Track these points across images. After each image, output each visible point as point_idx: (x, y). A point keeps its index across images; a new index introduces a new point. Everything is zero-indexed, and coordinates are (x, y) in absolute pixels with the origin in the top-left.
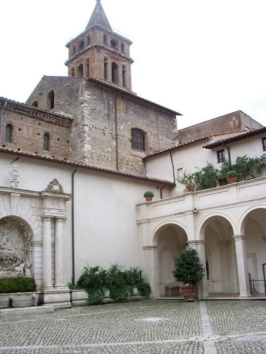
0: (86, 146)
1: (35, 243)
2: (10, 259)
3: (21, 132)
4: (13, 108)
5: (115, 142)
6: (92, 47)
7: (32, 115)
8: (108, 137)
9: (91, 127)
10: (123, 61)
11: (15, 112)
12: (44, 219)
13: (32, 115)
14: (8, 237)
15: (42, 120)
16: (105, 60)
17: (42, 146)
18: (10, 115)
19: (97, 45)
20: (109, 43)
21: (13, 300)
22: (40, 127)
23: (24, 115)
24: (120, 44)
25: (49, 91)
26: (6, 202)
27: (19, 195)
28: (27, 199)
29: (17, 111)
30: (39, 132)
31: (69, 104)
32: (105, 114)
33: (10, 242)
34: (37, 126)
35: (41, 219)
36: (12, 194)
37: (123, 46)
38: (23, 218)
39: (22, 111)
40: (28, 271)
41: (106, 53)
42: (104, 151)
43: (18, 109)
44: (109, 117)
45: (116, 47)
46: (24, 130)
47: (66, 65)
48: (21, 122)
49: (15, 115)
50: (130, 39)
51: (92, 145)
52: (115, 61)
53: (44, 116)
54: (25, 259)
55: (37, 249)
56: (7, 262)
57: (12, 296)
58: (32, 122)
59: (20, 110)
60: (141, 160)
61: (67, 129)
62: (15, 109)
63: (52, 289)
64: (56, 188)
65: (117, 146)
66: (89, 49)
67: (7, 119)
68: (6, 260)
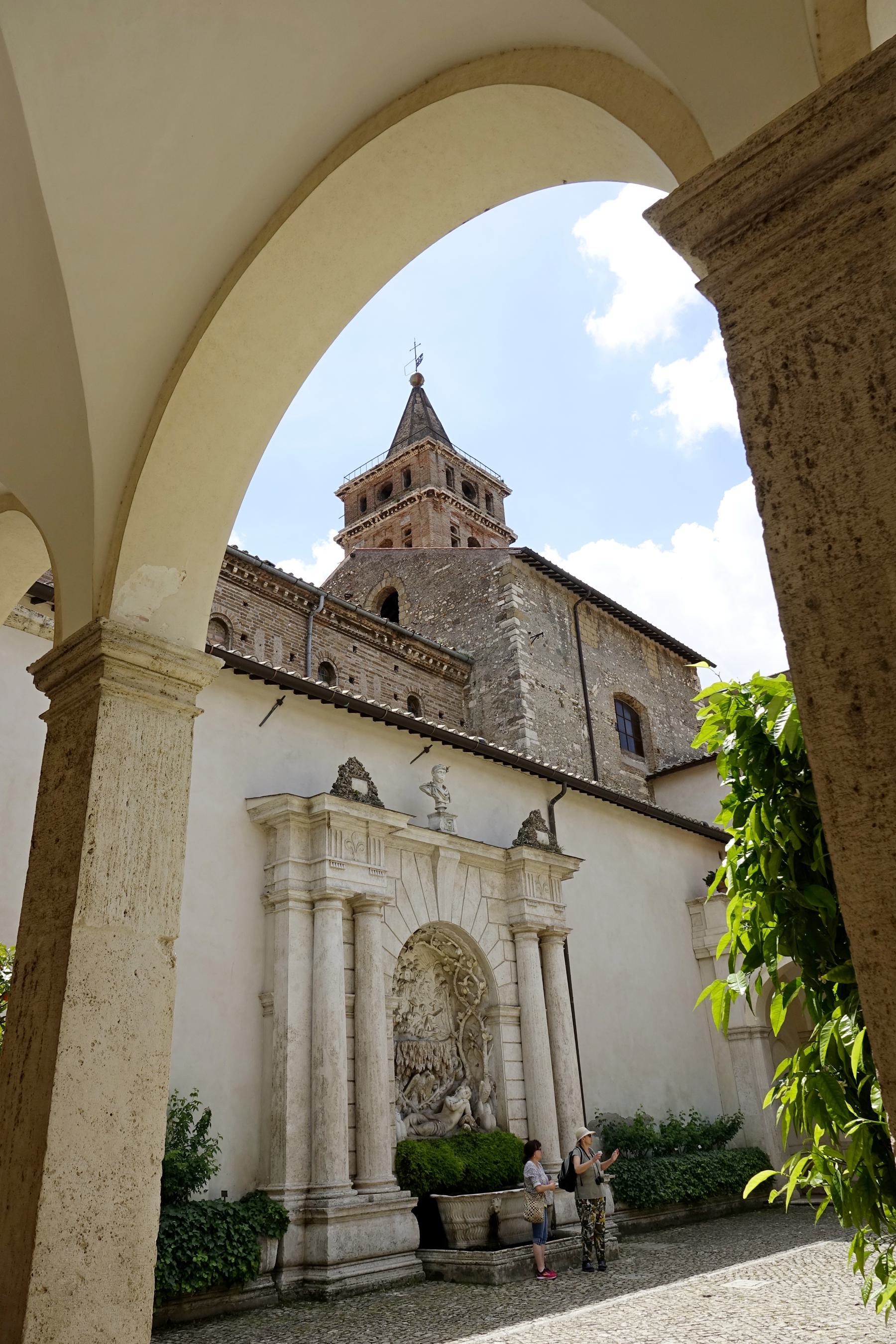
0: (529, 733)
5: (586, 727)
6: (420, 497)
7: (378, 641)
8: (568, 716)
9: (534, 682)
10: (494, 537)
11: (339, 630)
13: (378, 641)
15: (402, 658)
16: (453, 529)
18: (327, 638)
19: (433, 491)
20: (459, 487)
21: (500, 1216)
22: (398, 678)
24: (483, 494)
25: (379, 589)
27: (458, 856)
31: (456, 622)
32: (558, 651)
34: (390, 675)
37: (489, 498)
39: (355, 626)
40: (486, 1110)
41: (454, 514)
42: (565, 751)
43: (348, 623)
44: (566, 659)
45: (475, 501)
47: (339, 542)
48: (354, 659)
50: (508, 484)
51: (540, 734)
52: (474, 535)
53: (406, 648)
54: (463, 1069)
55: (508, 1033)
58: (378, 661)
60: (642, 780)
61: (457, 688)
62: (339, 620)
65: (591, 739)
66: (412, 500)
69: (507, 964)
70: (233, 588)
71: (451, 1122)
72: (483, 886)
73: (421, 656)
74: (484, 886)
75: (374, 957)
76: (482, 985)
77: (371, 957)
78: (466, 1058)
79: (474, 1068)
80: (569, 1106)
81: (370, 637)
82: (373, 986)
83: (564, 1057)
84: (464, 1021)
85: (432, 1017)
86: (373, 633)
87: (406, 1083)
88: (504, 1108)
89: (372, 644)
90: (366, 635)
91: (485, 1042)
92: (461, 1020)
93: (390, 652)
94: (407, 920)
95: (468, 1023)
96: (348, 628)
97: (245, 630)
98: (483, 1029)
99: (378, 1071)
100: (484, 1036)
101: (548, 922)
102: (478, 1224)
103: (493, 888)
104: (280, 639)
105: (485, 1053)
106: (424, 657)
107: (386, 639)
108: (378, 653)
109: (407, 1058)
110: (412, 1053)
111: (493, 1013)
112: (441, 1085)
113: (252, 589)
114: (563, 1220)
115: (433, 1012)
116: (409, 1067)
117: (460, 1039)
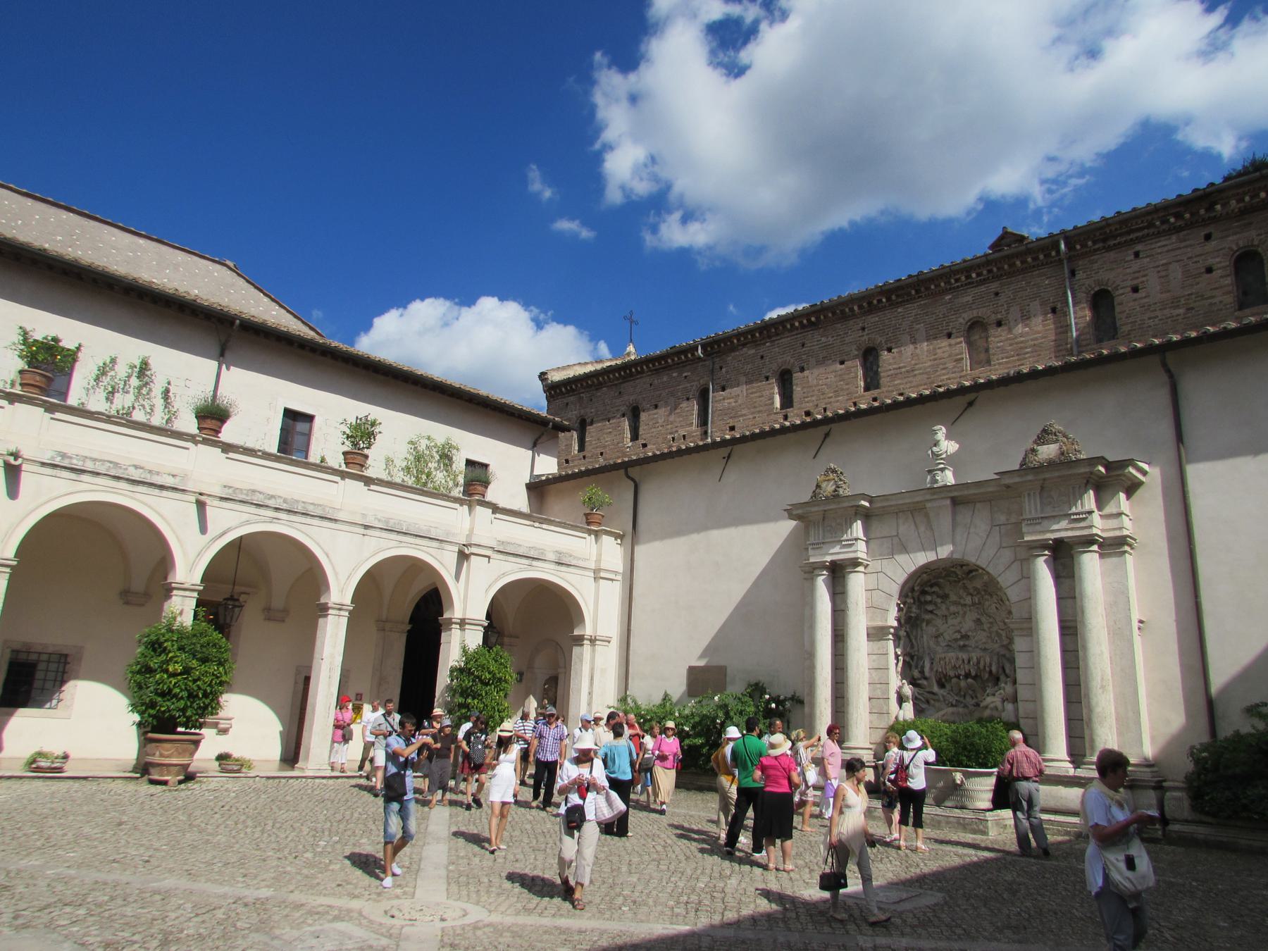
2: (967, 676)
3: (1141, 294)
4: (1095, 242)
11: (1109, 249)
13: (1165, 227)
15: (1215, 220)
17: (1229, 299)
18: (1095, 266)
22: (1213, 244)
23: (1139, 240)
26: (922, 529)
28: (978, 505)
29: (1111, 243)
30: (1210, 261)
33: (986, 626)
36: (928, 505)
39: (1129, 233)
43: (1115, 237)
46: (1153, 284)
48: (1136, 265)
49: (1112, 255)
53: (1210, 208)
59: (1121, 235)
62: (1104, 241)
63: (1068, 769)
64: (1048, 451)
67: (1087, 282)
70: (983, 288)
73: (1241, 200)
81: (1151, 231)
86: (1151, 225)
89: (1159, 234)
90: (1146, 231)
93: (1190, 226)
96: (1119, 240)
97: (999, 316)
104: (1037, 302)
106: (1247, 199)
107: (1172, 220)
108: (1174, 238)
113: (998, 277)
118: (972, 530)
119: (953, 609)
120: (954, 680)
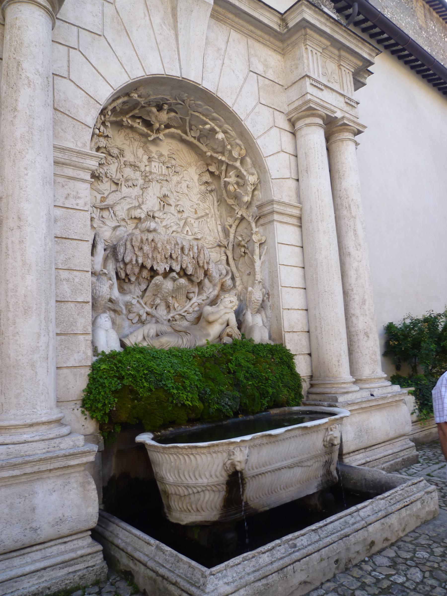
1: (276, 207)
2: (183, 273)
12: (299, 125)
14: (165, 191)
35: (287, 126)
38: (229, 101)
54: (233, 278)
55: (285, 234)
56: (168, 285)
57: (239, 457)
68: (166, 275)
69: (282, 154)
71: (208, 335)
72: (252, 59)
74: (254, 60)
75: (25, 65)
76: (252, 179)
77: (19, 64)
78: (237, 268)
79: (245, 278)
80: (361, 319)
82: (20, 107)
83: (355, 265)
84: (234, 227)
85: (193, 221)
87: (144, 287)
88: (279, 319)
91: (257, 245)
92: (231, 226)
94: (124, 61)
95: (239, 229)
98: (255, 229)
99: (21, 242)
100: (255, 238)
101: (339, 115)
102: (205, 488)
103: (266, 66)
105: (256, 257)
109: (140, 254)
110: (146, 248)
111: (267, 209)
112: (199, 293)
114: (352, 448)
115: (196, 216)
116: (143, 267)
117: (230, 247)
118: (227, 61)
119: (128, 172)
120: (158, 279)
